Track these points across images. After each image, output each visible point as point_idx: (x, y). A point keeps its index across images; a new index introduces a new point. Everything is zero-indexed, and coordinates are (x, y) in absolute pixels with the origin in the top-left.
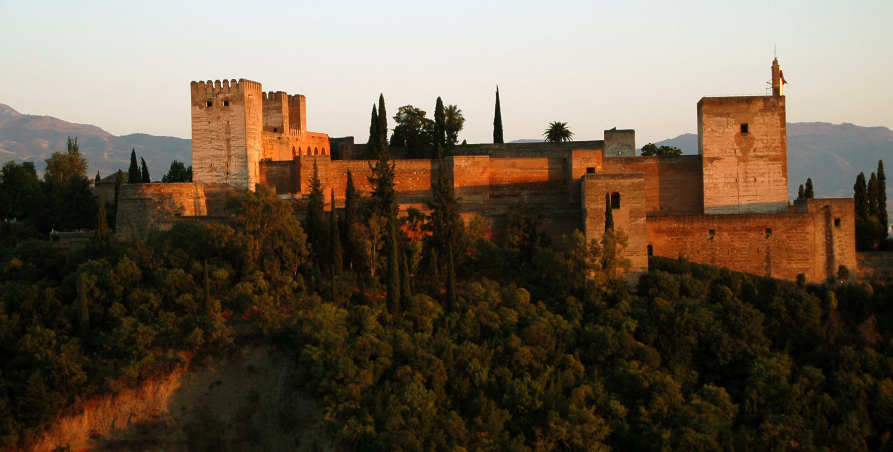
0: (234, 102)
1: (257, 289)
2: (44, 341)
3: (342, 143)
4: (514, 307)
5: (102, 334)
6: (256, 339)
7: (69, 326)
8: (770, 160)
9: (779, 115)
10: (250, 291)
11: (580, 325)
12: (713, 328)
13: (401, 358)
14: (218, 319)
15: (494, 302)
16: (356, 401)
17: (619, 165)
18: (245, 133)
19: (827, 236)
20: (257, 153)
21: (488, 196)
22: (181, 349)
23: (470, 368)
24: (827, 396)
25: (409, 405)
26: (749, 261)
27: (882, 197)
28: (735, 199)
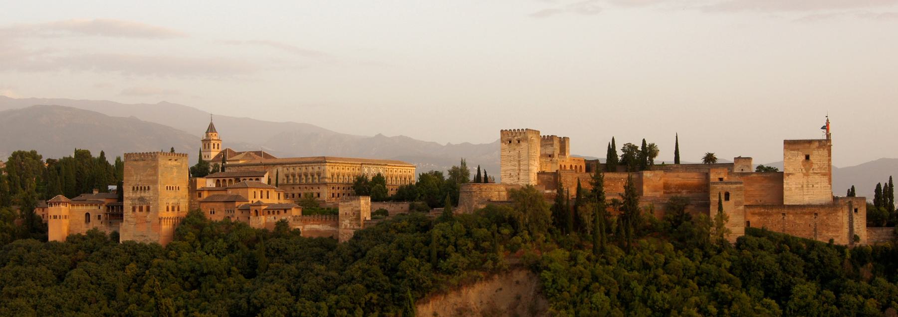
0: (523, 141)
1: (524, 240)
2: (413, 264)
3: (593, 163)
4: (663, 253)
5: (441, 261)
6: (519, 266)
7: (426, 257)
8: (822, 175)
9: (827, 150)
10: (520, 241)
11: (699, 264)
12: (773, 267)
13: (595, 278)
14: (501, 255)
15: (653, 250)
16: (566, 301)
17: (737, 177)
18: (529, 157)
19: (850, 218)
20: (536, 168)
21: (662, 193)
22: (481, 271)
23: (632, 286)
24: (834, 307)
25: (594, 304)
26: (805, 231)
27: (891, 196)
28: (801, 196)
